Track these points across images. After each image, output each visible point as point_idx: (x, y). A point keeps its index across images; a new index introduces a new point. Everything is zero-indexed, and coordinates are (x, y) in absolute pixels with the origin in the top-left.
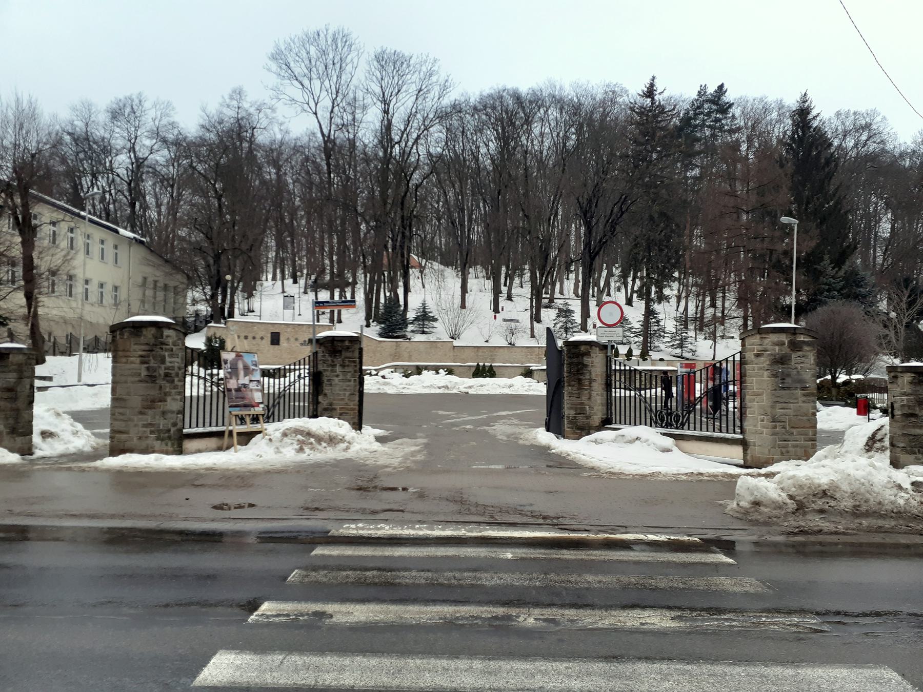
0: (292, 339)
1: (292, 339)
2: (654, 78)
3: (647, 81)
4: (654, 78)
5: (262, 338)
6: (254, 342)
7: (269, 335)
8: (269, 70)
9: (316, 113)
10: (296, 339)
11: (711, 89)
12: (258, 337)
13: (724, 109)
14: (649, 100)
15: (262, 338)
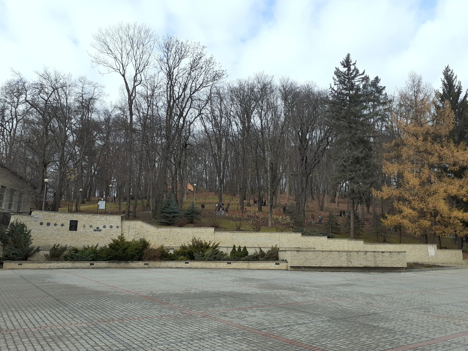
0: (87, 226)
1: (87, 226)
2: (348, 55)
3: (345, 56)
4: (348, 55)
5: (62, 225)
6: (55, 228)
7: (69, 222)
8: (94, 47)
9: (123, 76)
10: (91, 226)
11: (372, 78)
12: (59, 224)
13: (380, 90)
14: (346, 69)
15: (62, 225)
